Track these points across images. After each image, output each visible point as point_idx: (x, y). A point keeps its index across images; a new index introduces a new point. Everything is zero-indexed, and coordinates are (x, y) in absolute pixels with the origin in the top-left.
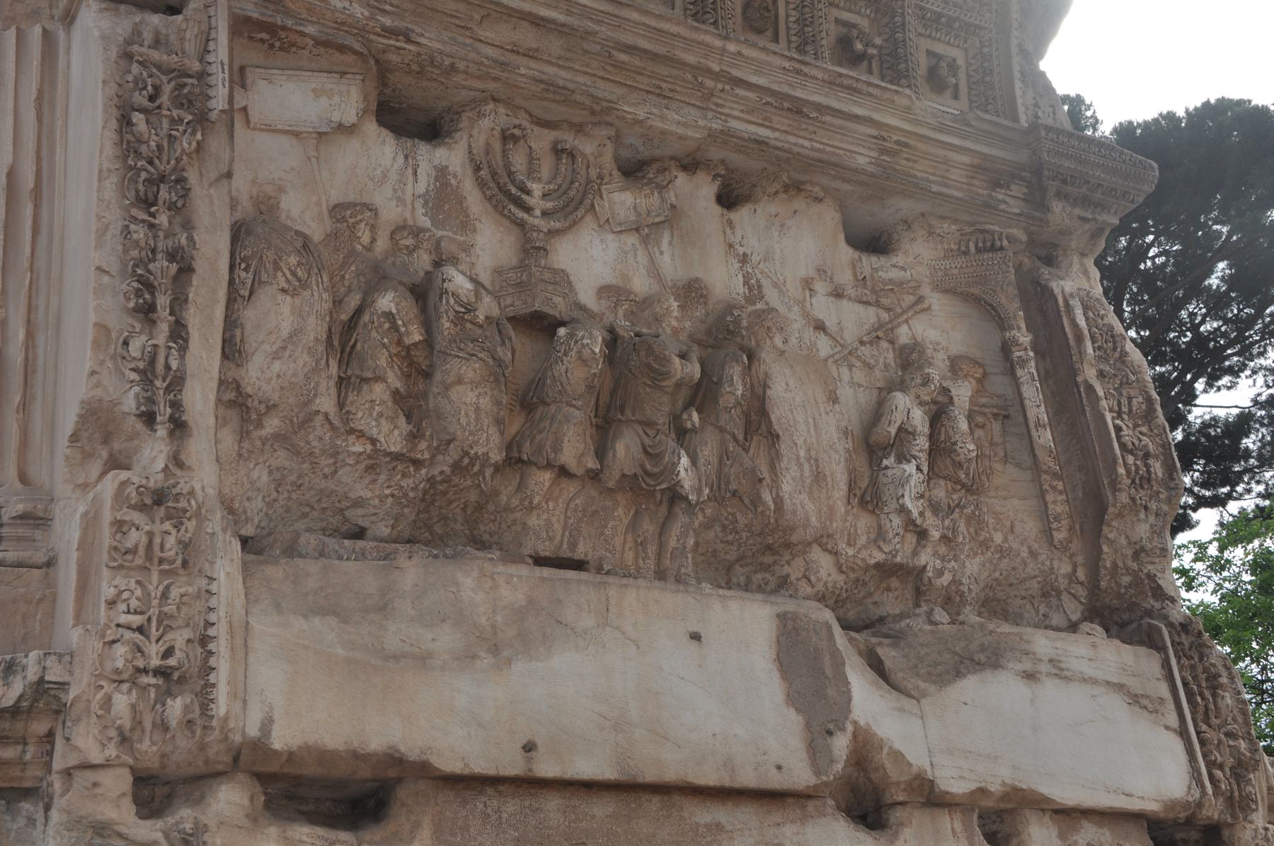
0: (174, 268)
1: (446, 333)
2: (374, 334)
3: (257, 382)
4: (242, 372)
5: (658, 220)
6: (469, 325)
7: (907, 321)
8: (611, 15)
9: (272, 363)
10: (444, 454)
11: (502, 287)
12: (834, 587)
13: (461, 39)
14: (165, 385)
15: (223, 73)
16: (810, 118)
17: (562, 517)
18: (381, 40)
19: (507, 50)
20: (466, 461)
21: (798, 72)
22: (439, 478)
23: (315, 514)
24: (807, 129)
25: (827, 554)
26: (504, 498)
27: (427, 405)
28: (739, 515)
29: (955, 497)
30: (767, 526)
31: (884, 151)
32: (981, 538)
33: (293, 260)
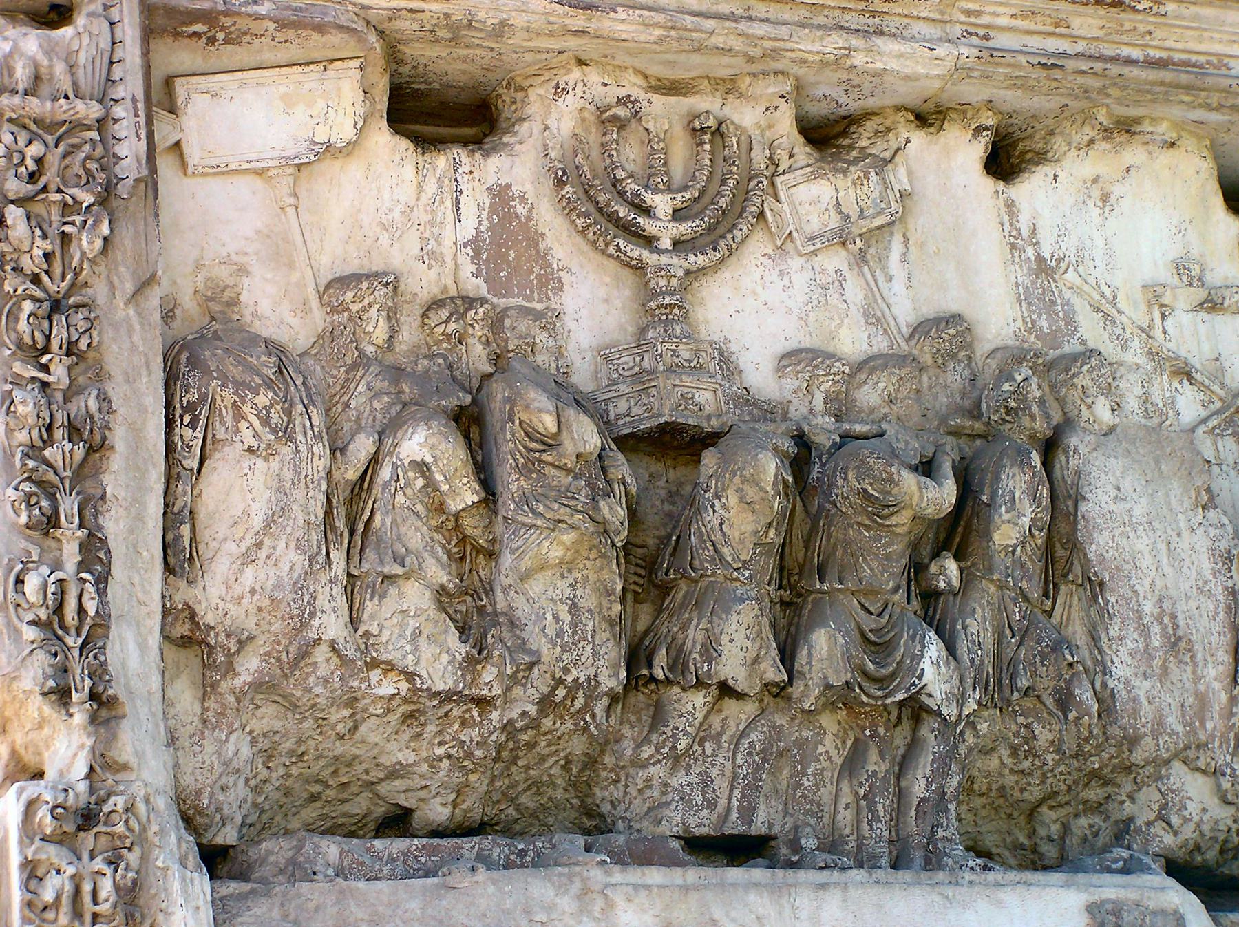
0: (80, 452)
1: (514, 487)
2: (400, 499)
3: (221, 604)
4: (197, 591)
5: (878, 222)
6: (553, 472)
9: (241, 571)
10: (524, 685)
11: (613, 382)
12: (1212, 830)
14: (80, 641)
15: (136, 115)
16: (1138, 11)
17: (729, 765)
20: (561, 693)
23: (331, 793)
24: (1135, 29)
25: (1198, 775)
26: (628, 747)
27: (494, 604)
30: (1087, 740)
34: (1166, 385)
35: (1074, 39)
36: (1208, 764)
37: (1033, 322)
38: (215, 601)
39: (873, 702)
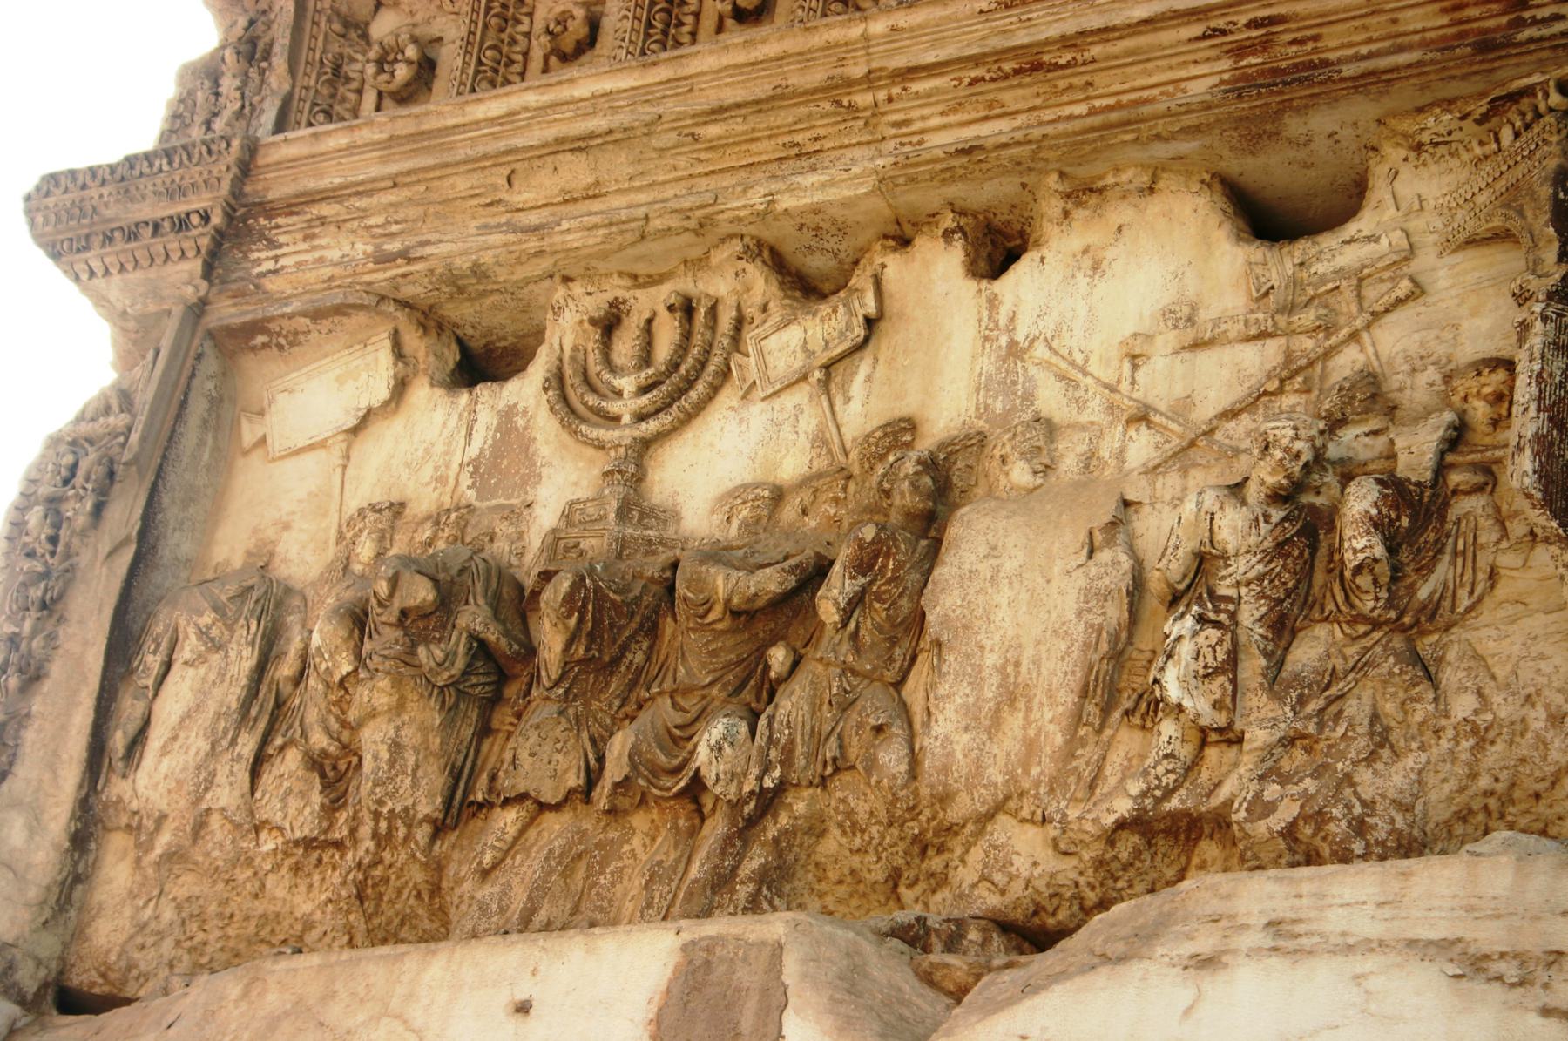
5: (839, 350)
7: (1354, 336)
8: (678, 80)
9: (159, 762)
12: (1048, 885)
13: (492, 221)
16: (1062, 67)
17: (530, 873)
18: (380, 276)
19: (559, 203)
20: (383, 825)
22: (366, 861)
24: (1071, 87)
25: (1027, 826)
28: (853, 802)
31: (1238, 51)
32: (1418, 717)
33: (207, 618)
34: (1118, 436)
36: (1033, 813)
37: (987, 407)
38: (141, 790)
39: (666, 794)
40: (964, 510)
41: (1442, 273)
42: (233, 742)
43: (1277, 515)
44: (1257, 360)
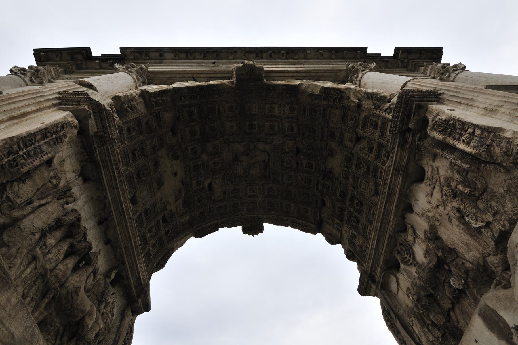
7: (439, 177)
16: (391, 192)
21: (382, 194)
29: (484, 200)
35: (395, 199)
40: (439, 233)
41: (436, 164)
42: (425, 331)
43: (457, 199)
44: (437, 190)
